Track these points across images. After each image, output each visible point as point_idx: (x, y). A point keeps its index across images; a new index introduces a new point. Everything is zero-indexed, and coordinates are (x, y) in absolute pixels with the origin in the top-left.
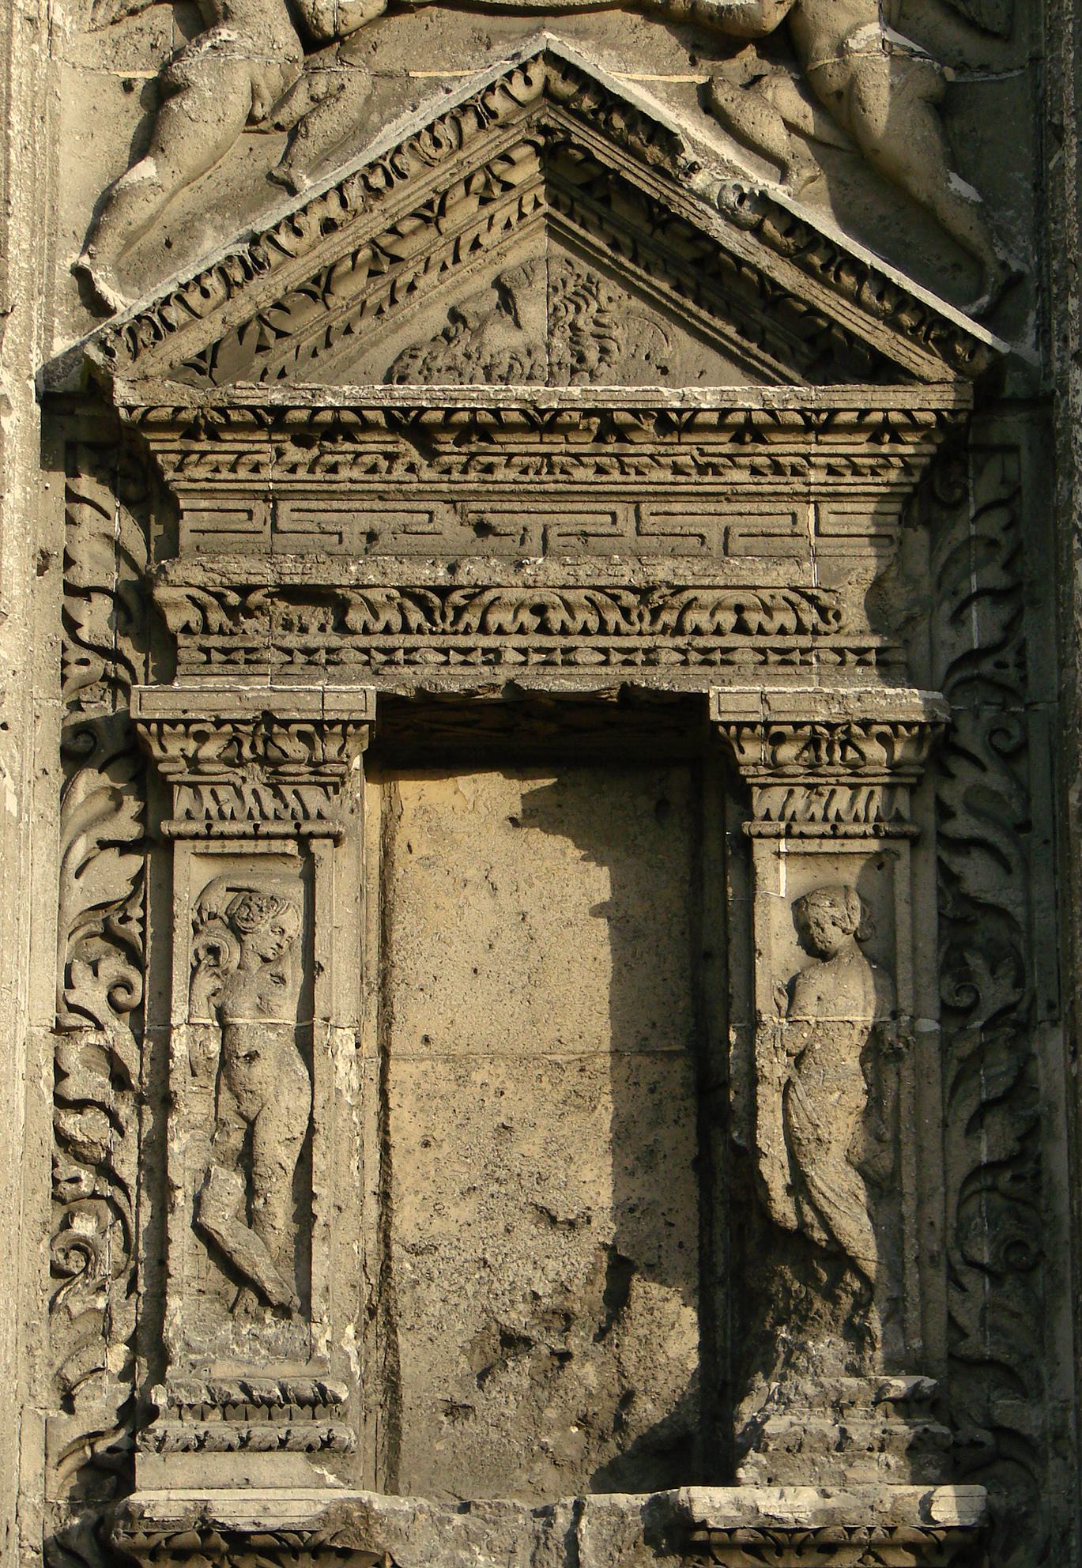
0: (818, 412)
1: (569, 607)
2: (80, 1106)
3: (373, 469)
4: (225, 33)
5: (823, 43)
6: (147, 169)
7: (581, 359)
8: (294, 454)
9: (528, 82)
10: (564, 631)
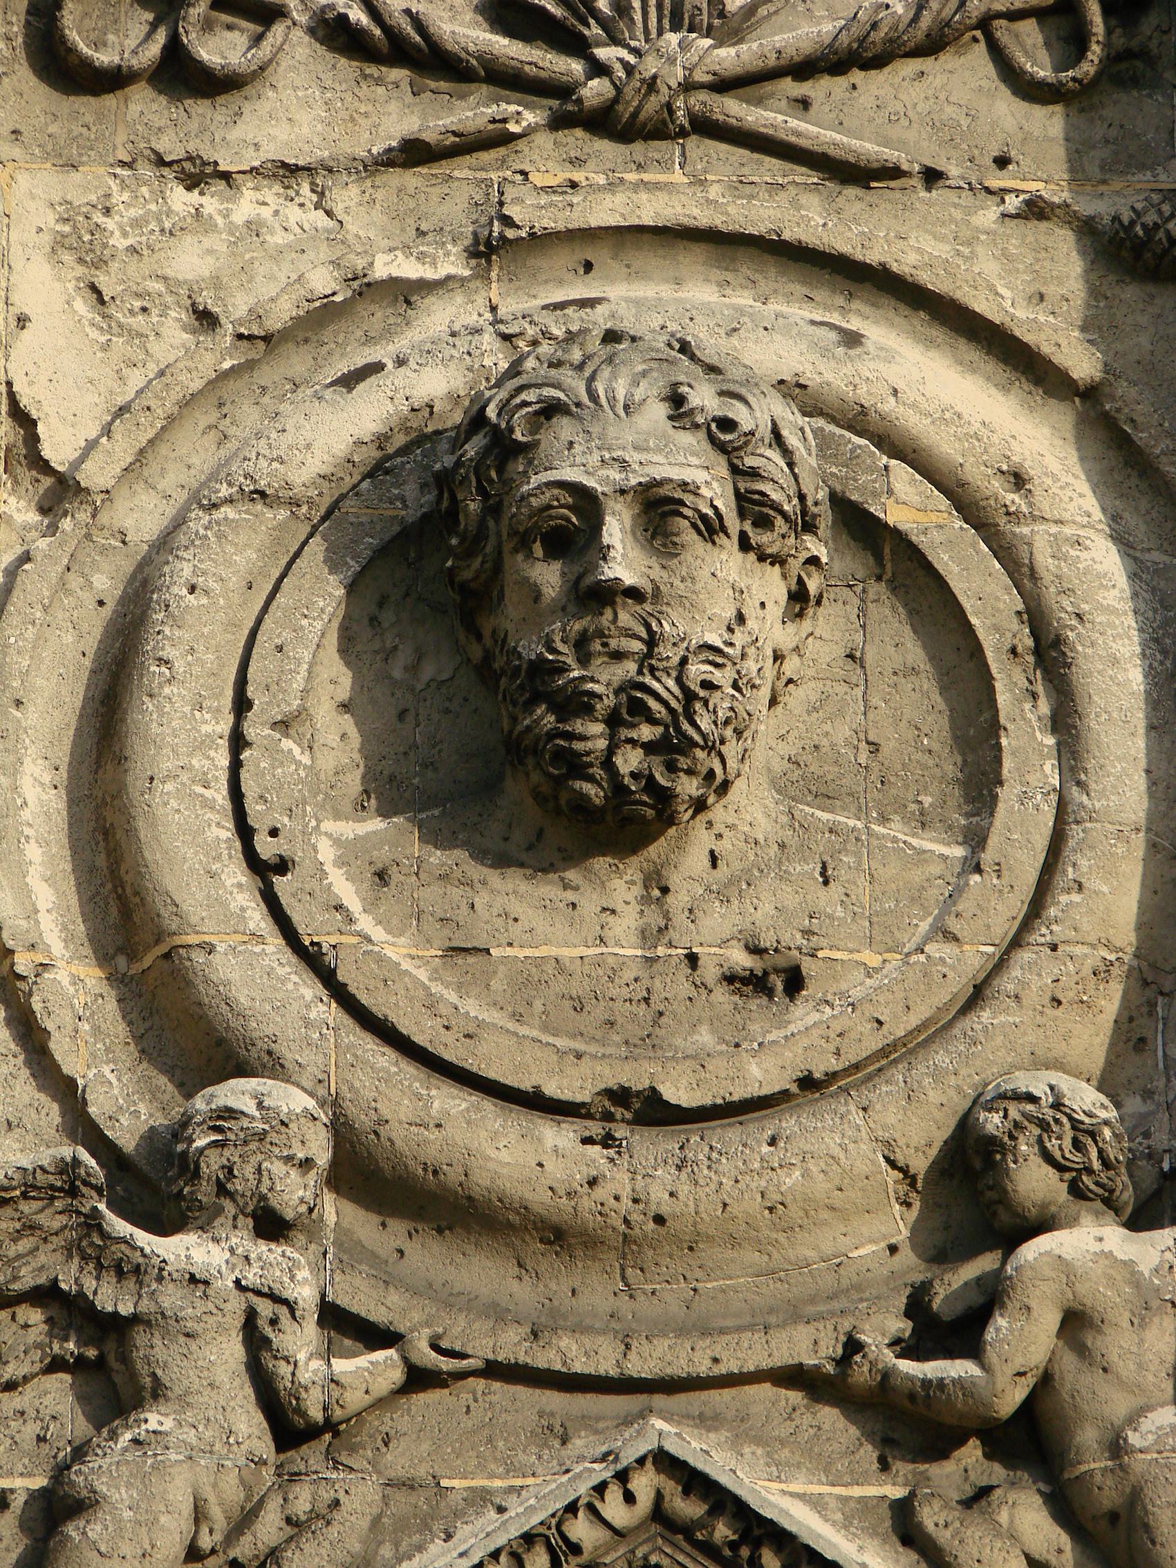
4: (154, 1419)
5: (1088, 1437)
9: (629, 1498)
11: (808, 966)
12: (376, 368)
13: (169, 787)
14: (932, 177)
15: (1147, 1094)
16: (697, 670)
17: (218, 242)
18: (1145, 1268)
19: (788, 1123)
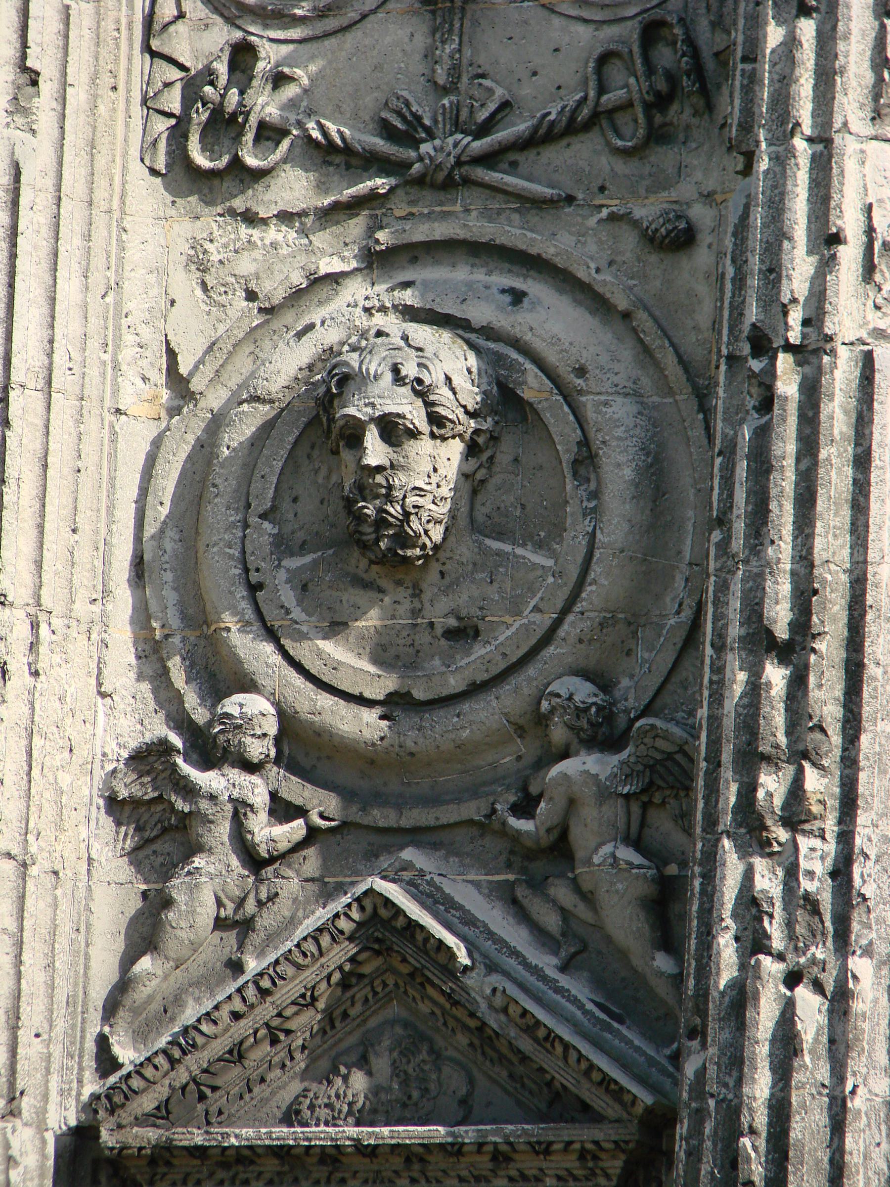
0: (539, 1143)
6: (145, 963)
7: (410, 1097)
8: (221, 1174)
11: (482, 626)
12: (311, 327)
13: (215, 549)
14: (570, 199)
15: (632, 676)
16: (411, 500)
17: (257, 254)
18: (602, 777)
19: (466, 707)
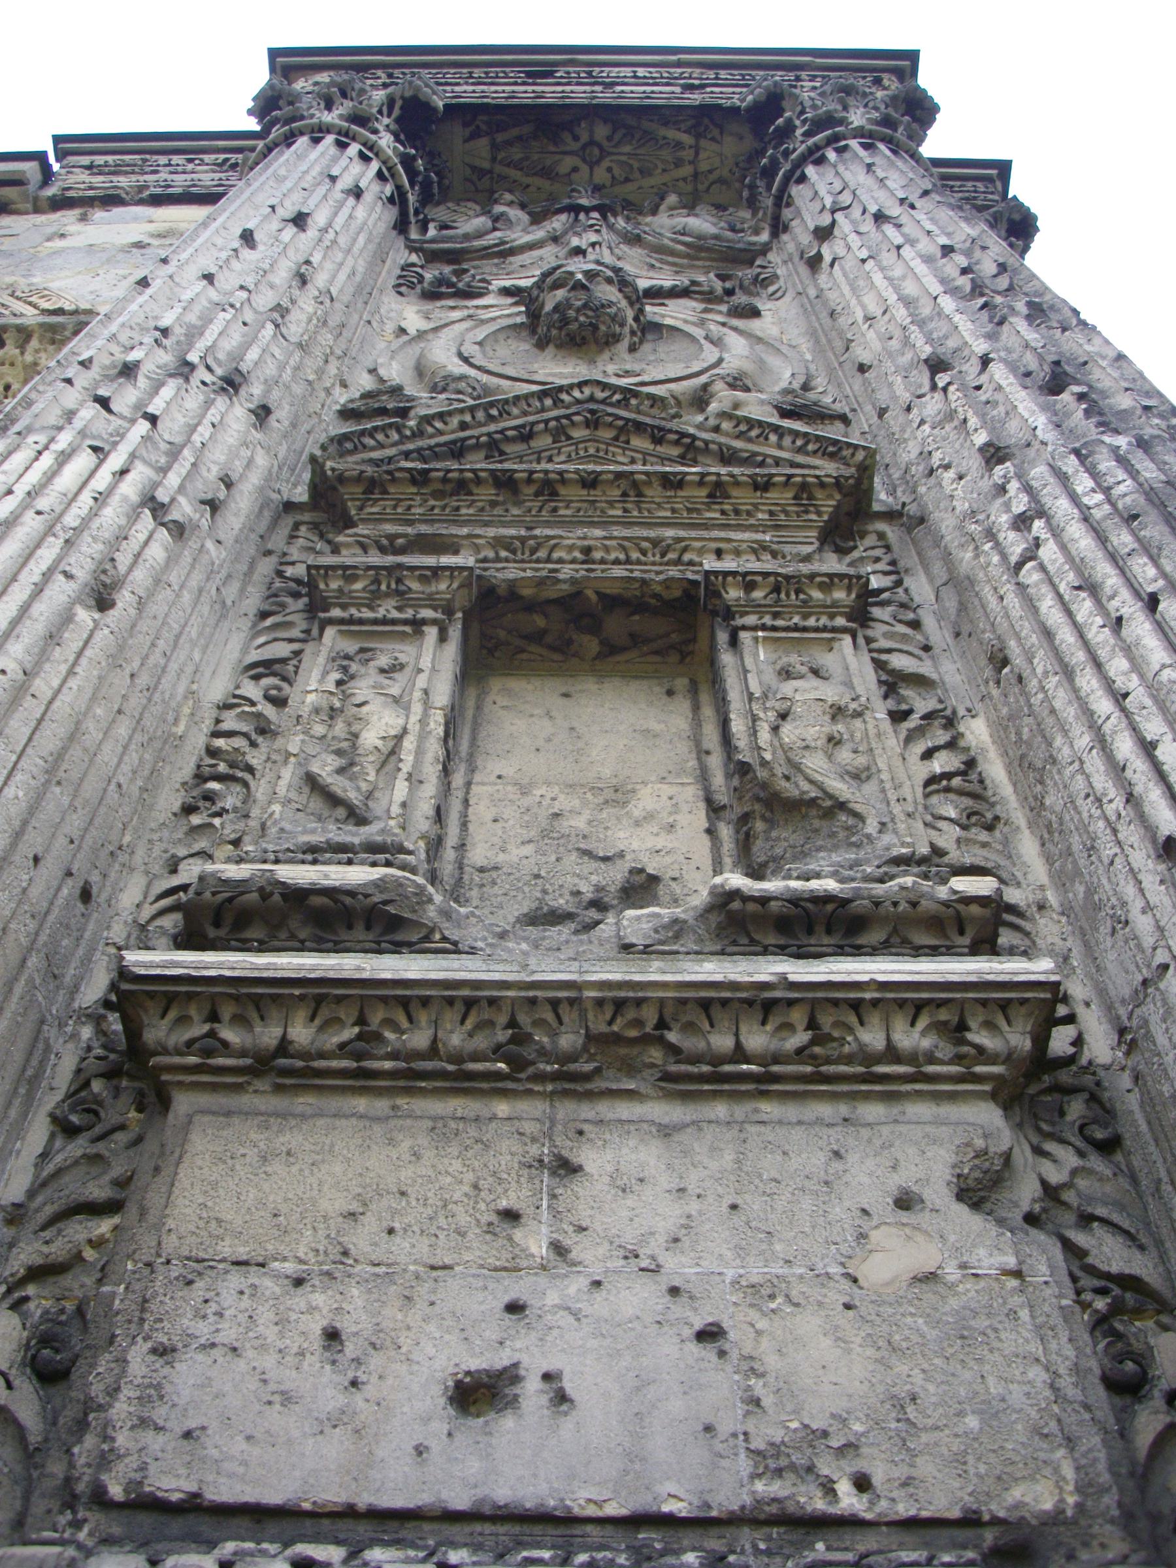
1: (607, 549)
2: (230, 734)
3: (482, 509)
10: (603, 561)
